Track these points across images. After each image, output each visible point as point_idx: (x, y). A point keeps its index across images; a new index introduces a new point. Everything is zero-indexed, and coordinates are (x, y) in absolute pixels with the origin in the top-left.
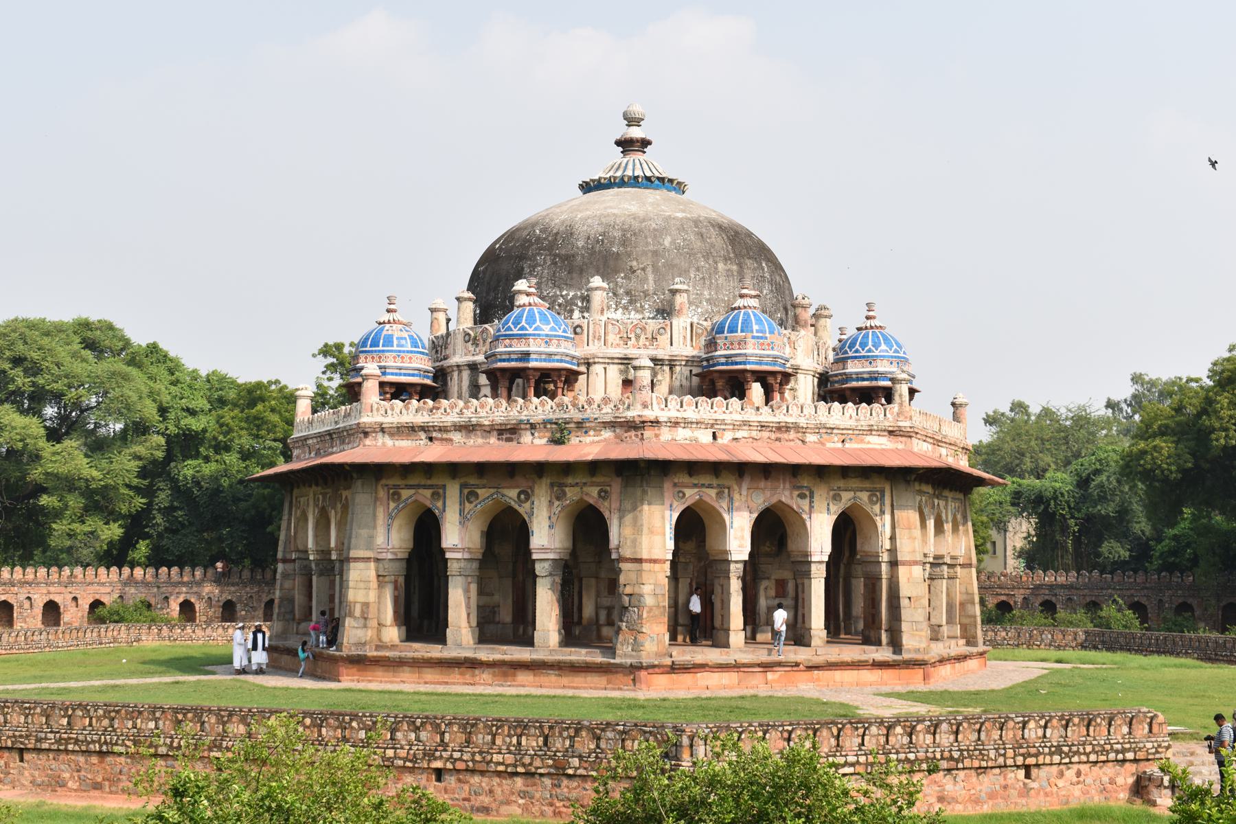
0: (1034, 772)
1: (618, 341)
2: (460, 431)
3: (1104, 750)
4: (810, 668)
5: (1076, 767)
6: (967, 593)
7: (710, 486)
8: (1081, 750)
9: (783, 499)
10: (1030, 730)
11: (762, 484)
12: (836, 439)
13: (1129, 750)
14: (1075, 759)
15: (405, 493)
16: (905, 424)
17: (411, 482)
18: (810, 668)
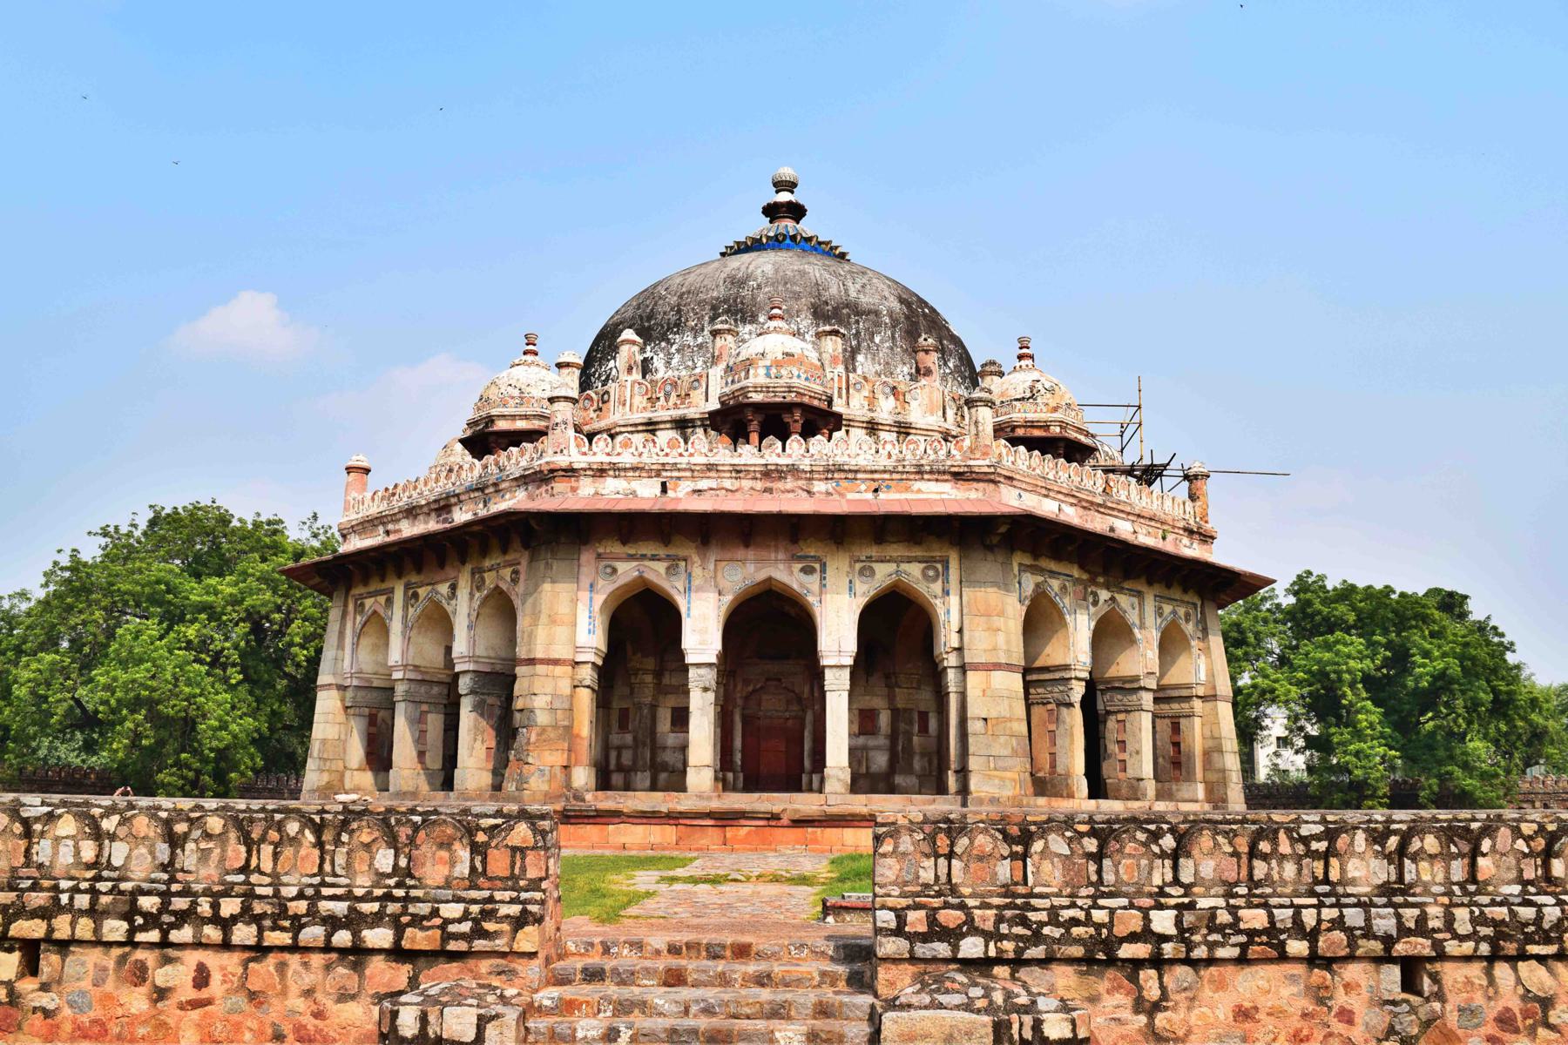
0: (49, 962)
1: (645, 403)
2: (407, 517)
3: (283, 912)
4: (800, 823)
5: (192, 958)
6: (1213, 738)
7: (654, 558)
8: (205, 908)
9: (773, 575)
10: (57, 840)
11: (741, 553)
12: (863, 487)
13: (376, 920)
14: (184, 934)
15: (369, 602)
16: (981, 464)
17: (372, 588)
18: (800, 823)
